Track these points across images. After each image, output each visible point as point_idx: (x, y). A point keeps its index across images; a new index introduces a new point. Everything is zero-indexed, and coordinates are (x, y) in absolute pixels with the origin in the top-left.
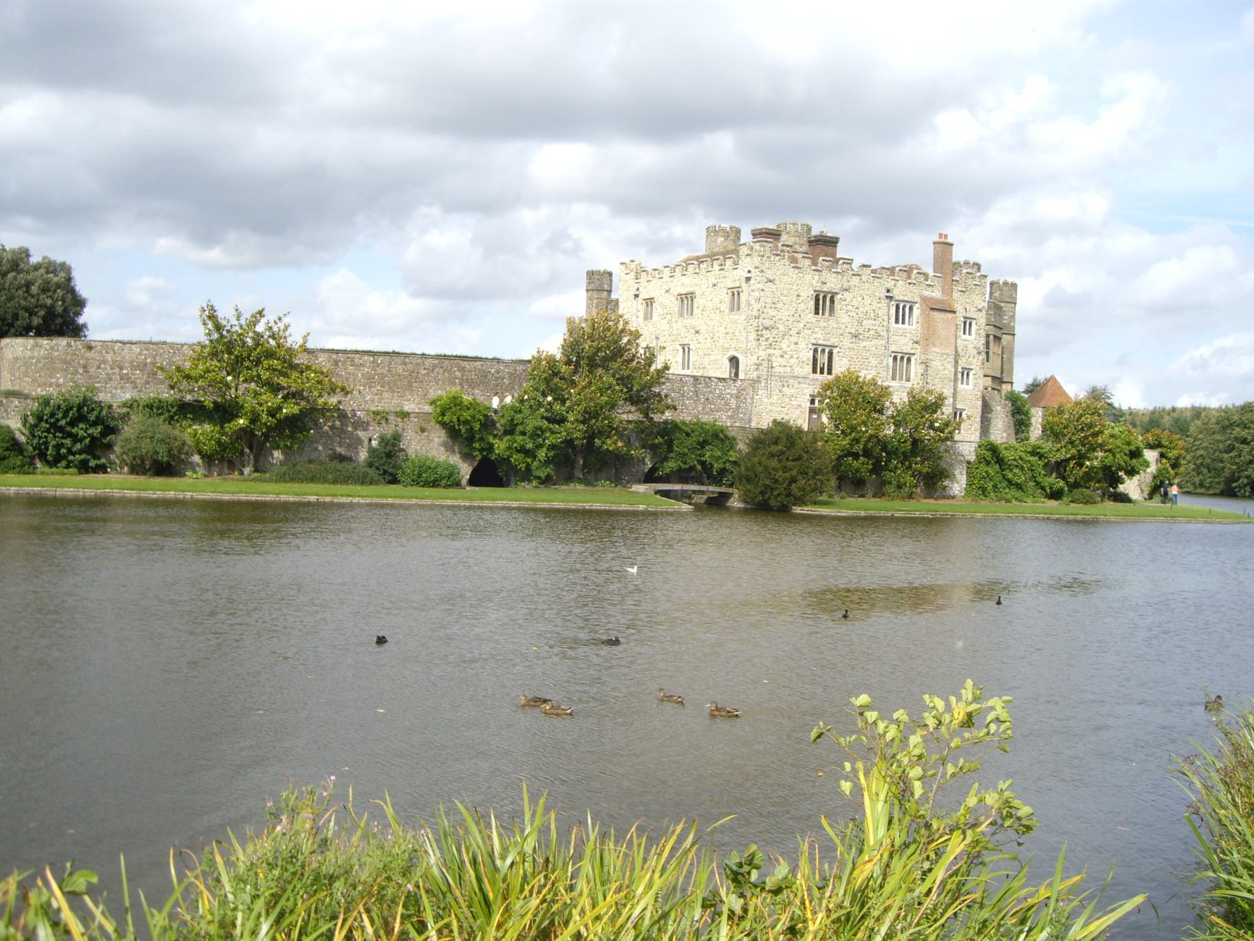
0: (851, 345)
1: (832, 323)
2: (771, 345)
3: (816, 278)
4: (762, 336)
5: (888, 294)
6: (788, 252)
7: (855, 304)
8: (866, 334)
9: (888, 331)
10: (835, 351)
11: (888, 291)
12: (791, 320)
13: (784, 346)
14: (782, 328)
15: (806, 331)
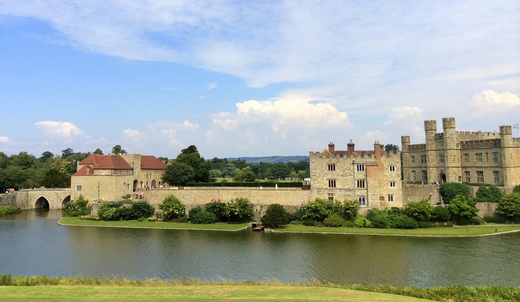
0: (341, 179)
1: (334, 172)
2: (314, 180)
3: (328, 160)
4: (312, 178)
5: (354, 163)
6: (318, 154)
7: (342, 166)
8: (346, 175)
9: (354, 173)
10: (336, 180)
11: (354, 161)
12: (321, 172)
13: (319, 180)
14: (317, 175)
15: (325, 176)
